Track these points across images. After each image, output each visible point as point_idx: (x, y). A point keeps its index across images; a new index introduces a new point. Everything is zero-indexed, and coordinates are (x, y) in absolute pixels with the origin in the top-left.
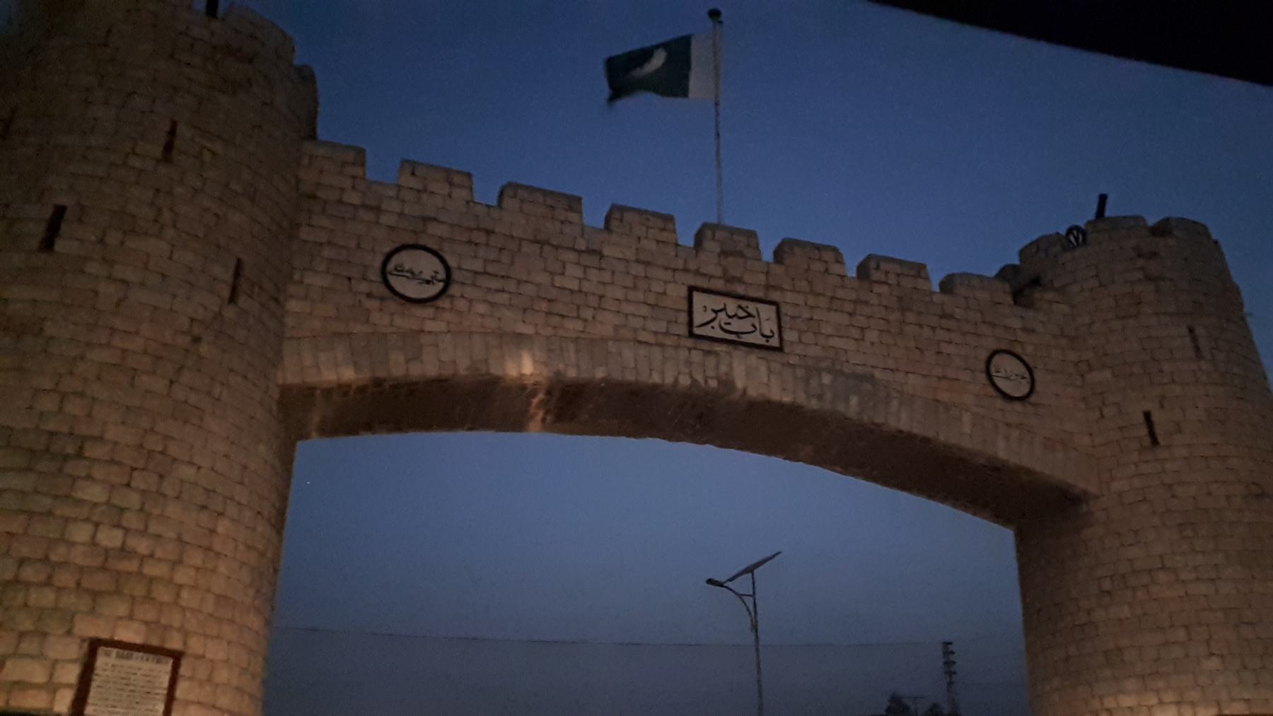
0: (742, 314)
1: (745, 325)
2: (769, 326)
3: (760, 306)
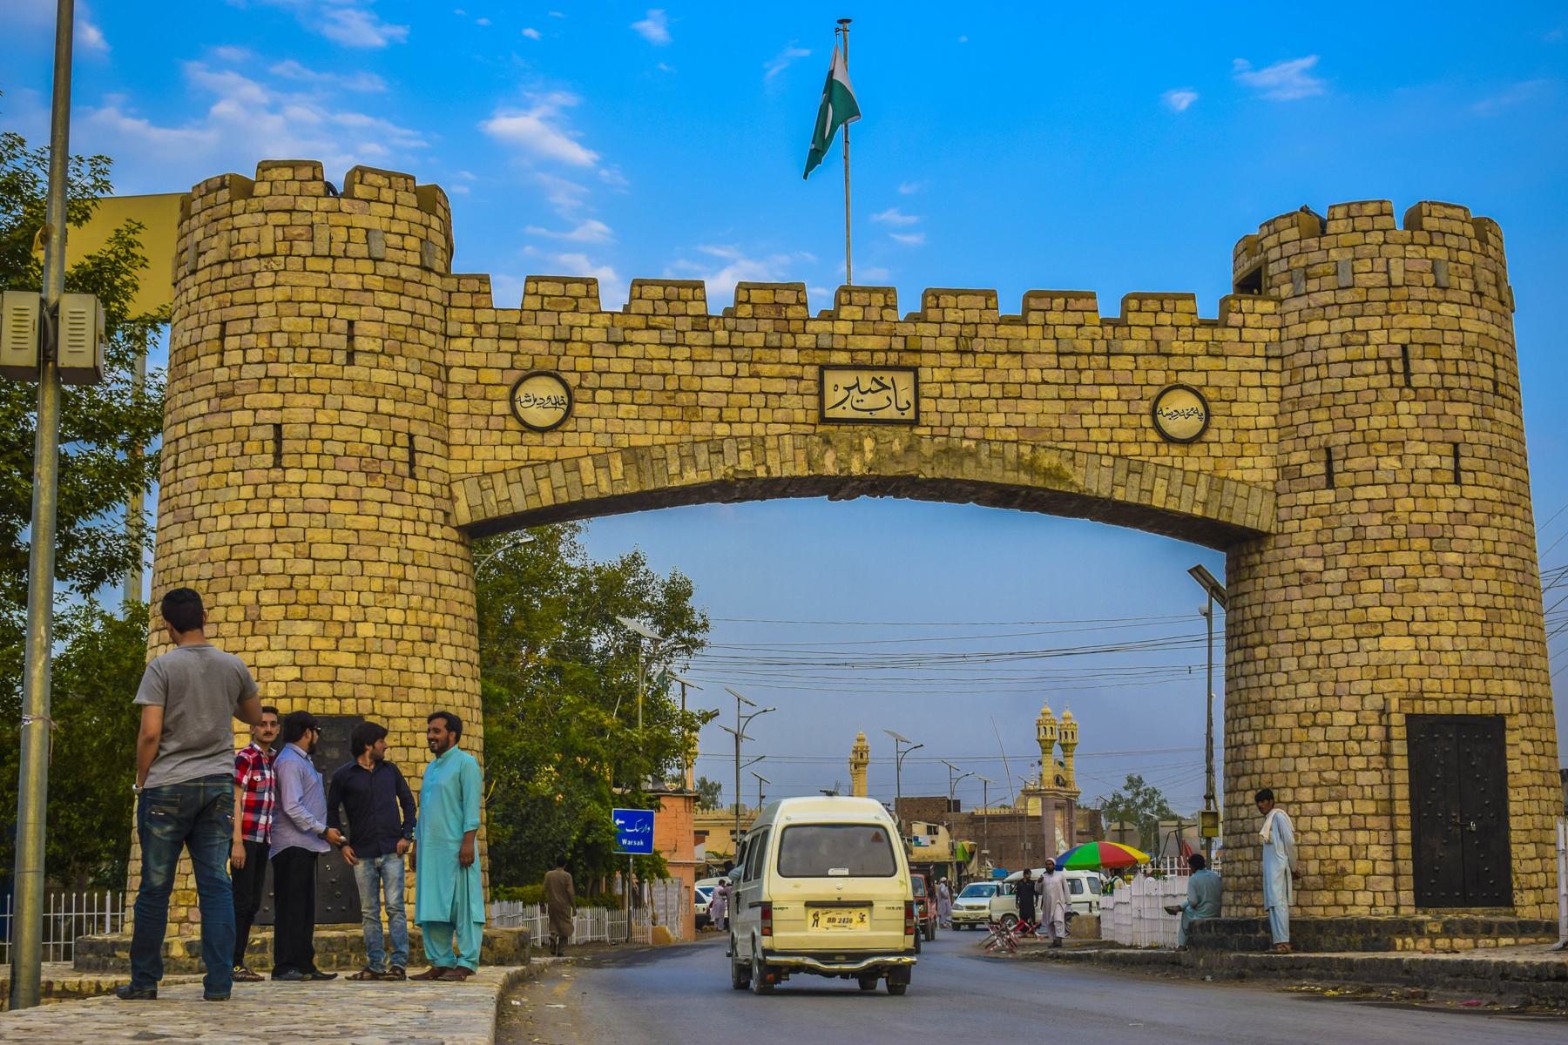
0: (876, 387)
1: (880, 399)
2: (906, 395)
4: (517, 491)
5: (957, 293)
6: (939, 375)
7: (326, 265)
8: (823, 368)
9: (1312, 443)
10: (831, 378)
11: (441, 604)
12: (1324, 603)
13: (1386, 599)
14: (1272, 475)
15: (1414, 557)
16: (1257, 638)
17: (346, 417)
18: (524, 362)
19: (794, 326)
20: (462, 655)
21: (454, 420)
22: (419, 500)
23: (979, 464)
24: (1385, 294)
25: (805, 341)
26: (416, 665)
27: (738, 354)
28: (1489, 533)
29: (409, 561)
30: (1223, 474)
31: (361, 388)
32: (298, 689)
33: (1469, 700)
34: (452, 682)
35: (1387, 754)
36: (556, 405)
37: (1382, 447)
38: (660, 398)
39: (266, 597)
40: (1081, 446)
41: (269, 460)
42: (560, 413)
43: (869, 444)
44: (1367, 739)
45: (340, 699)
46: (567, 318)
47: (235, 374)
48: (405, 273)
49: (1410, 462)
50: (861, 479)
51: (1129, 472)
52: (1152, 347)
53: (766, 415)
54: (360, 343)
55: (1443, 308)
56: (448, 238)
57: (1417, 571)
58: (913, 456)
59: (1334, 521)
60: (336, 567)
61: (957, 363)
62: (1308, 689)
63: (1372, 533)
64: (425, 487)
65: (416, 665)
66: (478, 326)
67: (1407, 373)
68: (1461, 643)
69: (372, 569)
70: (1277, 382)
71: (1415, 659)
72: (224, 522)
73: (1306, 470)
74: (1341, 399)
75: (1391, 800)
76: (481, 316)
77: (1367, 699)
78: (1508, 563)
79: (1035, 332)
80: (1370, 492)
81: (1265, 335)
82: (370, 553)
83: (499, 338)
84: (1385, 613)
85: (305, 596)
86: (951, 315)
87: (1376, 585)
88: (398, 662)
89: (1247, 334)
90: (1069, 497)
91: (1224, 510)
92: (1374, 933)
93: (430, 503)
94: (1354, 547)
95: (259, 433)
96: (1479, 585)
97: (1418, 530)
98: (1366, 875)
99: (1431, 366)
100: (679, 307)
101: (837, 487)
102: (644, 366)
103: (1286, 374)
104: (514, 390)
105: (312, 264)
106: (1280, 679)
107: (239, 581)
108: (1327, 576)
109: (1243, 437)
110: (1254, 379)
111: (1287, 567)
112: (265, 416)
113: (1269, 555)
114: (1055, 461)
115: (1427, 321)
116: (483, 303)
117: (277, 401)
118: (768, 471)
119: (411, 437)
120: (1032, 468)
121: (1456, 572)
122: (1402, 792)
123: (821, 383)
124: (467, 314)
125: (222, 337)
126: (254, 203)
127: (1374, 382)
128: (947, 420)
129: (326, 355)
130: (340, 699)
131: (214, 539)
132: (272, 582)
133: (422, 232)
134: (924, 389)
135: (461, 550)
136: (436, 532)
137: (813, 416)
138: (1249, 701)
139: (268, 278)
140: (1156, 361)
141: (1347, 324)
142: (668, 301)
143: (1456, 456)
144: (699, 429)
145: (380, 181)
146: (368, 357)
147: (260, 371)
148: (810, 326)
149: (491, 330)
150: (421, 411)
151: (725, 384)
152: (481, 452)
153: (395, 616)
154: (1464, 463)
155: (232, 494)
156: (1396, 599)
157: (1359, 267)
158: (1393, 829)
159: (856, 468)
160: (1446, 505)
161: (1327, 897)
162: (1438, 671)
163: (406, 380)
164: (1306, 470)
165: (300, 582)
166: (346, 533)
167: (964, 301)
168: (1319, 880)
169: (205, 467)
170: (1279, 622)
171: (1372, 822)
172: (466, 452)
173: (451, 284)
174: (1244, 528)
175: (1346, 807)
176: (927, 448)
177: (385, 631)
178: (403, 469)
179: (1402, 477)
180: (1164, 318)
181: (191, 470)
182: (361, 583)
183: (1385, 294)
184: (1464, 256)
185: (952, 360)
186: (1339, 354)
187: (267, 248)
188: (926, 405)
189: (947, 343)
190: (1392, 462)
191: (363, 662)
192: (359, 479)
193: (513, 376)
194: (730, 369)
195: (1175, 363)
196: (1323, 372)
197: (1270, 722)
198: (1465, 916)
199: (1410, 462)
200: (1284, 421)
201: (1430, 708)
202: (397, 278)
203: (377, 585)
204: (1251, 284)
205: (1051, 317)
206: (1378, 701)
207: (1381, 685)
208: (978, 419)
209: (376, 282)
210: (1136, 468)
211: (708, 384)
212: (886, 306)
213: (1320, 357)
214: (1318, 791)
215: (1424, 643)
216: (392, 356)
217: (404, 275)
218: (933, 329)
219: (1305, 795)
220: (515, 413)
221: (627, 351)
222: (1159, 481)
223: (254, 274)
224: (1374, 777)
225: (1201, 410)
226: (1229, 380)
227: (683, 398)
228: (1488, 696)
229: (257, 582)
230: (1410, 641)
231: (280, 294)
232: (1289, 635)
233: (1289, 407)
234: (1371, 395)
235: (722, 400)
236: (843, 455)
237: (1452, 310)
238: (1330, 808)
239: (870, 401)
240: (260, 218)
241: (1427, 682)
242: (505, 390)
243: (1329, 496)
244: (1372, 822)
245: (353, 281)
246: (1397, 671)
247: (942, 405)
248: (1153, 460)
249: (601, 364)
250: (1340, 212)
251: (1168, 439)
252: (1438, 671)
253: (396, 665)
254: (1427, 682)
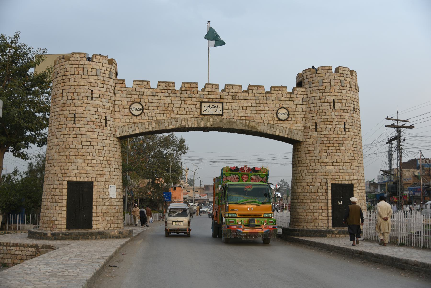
1: (214, 110)
2: (220, 109)
3: (218, 104)
4: (130, 129)
5: (232, 85)
6: (228, 104)
7: (87, 77)
8: (201, 102)
9: (312, 121)
10: (203, 104)
11: (112, 155)
12: (314, 158)
13: (328, 157)
14: (303, 128)
15: (334, 148)
16: (299, 165)
17: (90, 112)
18: (133, 100)
19: (195, 92)
20: (117, 167)
21: (116, 113)
22: (107, 132)
23: (236, 125)
24: (330, 88)
25: (197, 96)
26: (106, 169)
27: (182, 99)
28: (351, 143)
29: (105, 145)
31: (94, 106)
32: (79, 175)
33: (346, 180)
34: (115, 173)
35: (327, 193)
36: (140, 110)
37: (328, 123)
38: (164, 109)
39: (71, 154)
40: (260, 121)
41: (72, 122)
42: (141, 112)
43: (211, 120)
44: (322, 189)
45: (88, 177)
46: (143, 90)
47: (65, 102)
48: (105, 79)
49: (334, 126)
50: (210, 128)
51: (271, 127)
52: (277, 99)
53: (188, 113)
54: (94, 95)
55: (343, 91)
56: (116, 71)
57: (335, 151)
58: (222, 123)
59: (317, 139)
60: (87, 147)
61: (232, 102)
62: (310, 177)
63: (325, 142)
64: (109, 128)
65: (106, 169)
66: (122, 91)
67: (334, 106)
68: (344, 168)
69: (96, 147)
70: (305, 107)
71: (334, 171)
72: (62, 136)
73: (311, 127)
74: (319, 111)
75: (327, 203)
76: (123, 89)
77: (323, 180)
78: (355, 149)
79: (250, 95)
80: (325, 133)
81: (302, 96)
82: (95, 144)
83: (127, 94)
84: (327, 160)
85: (80, 154)
86: (231, 91)
87: (326, 154)
88: (102, 169)
89: (298, 96)
90: (257, 132)
91: (292, 136)
92: (322, 234)
93: (110, 132)
94: (321, 145)
95: (70, 116)
96: (349, 154)
97: (335, 142)
98: (321, 220)
99: (340, 104)
100: (169, 88)
101: (206, 129)
102: (160, 101)
103: (307, 105)
104: (130, 106)
105: (83, 77)
106: (304, 175)
107: (65, 150)
108: (315, 152)
109: (297, 119)
110: (300, 106)
111: (306, 149)
112: (72, 112)
113: (302, 146)
114: (254, 124)
115: (339, 94)
116: (123, 86)
117: (74, 108)
118: (188, 126)
119: (106, 117)
120: (248, 126)
121: (344, 151)
122: (330, 201)
123: (201, 106)
124: (120, 89)
125: (62, 93)
126: (70, 62)
127: (327, 108)
128: (230, 115)
129: (86, 98)
130: (88, 177)
131: (60, 140)
132: (73, 150)
133: (109, 70)
134: (224, 107)
135: (118, 143)
136: (111, 139)
137: (199, 113)
138: (297, 179)
139: (73, 80)
140: (277, 102)
141: (321, 94)
142: (166, 86)
143: (345, 125)
144: (172, 116)
145: (100, 57)
146: (96, 99)
147: (71, 101)
148: (199, 92)
149: (125, 92)
150: (108, 111)
151: (179, 106)
152: (122, 121)
153: (101, 158)
154: (346, 127)
155: (64, 129)
156: (330, 157)
157: (324, 81)
158: (328, 209)
159: (209, 125)
160: (342, 136)
161: (312, 224)
162: (339, 174)
163: (105, 104)
164: (311, 127)
165: (79, 150)
166: (90, 139)
167: (234, 87)
168: (311, 220)
169: (58, 123)
170: (304, 162)
171: (323, 208)
172: (119, 120)
173: (116, 82)
174: (296, 140)
175: (317, 204)
176: (225, 121)
177: (99, 162)
178: (104, 124)
179: (332, 130)
180: (280, 92)
181: (55, 124)
182: (93, 151)
183: (330, 88)
184: (348, 79)
185: (231, 101)
186: (319, 101)
187: (73, 73)
188: (225, 111)
189: (230, 97)
190: (330, 126)
191: (93, 169)
192: (93, 127)
193: (130, 103)
194: (180, 102)
195: (282, 102)
196: (315, 105)
197: (301, 184)
198: (343, 229)
199: (334, 126)
200: (306, 116)
201: (337, 182)
203: (97, 151)
204: (300, 84)
205: (254, 91)
206: (325, 180)
207: (326, 177)
208: (237, 114)
209: (98, 81)
210: (272, 126)
211: (175, 105)
212: (216, 88)
213: (315, 101)
214: (311, 200)
215: (336, 167)
216: (101, 98)
217: (105, 80)
218: (227, 94)
219: (308, 201)
220: (130, 112)
221: (156, 97)
222: (277, 129)
223: (70, 79)
224: (324, 198)
225: (287, 113)
226: (294, 106)
227: (169, 109)
228: (350, 180)
229: (69, 150)
230: (333, 167)
231: (76, 83)
232: (306, 165)
233: (307, 113)
234: (326, 111)
235: (178, 109)
236: (205, 122)
237: (345, 91)
238: (314, 204)
239: (212, 110)
240: (71, 66)
241: (336, 176)
242: (128, 106)
243: (316, 133)
244: (323, 208)
245: (93, 81)
246: (330, 174)
247: (229, 111)
249: (150, 101)
250: (320, 69)
251: (280, 120)
252: (339, 174)
253: (101, 170)
254: (336, 176)
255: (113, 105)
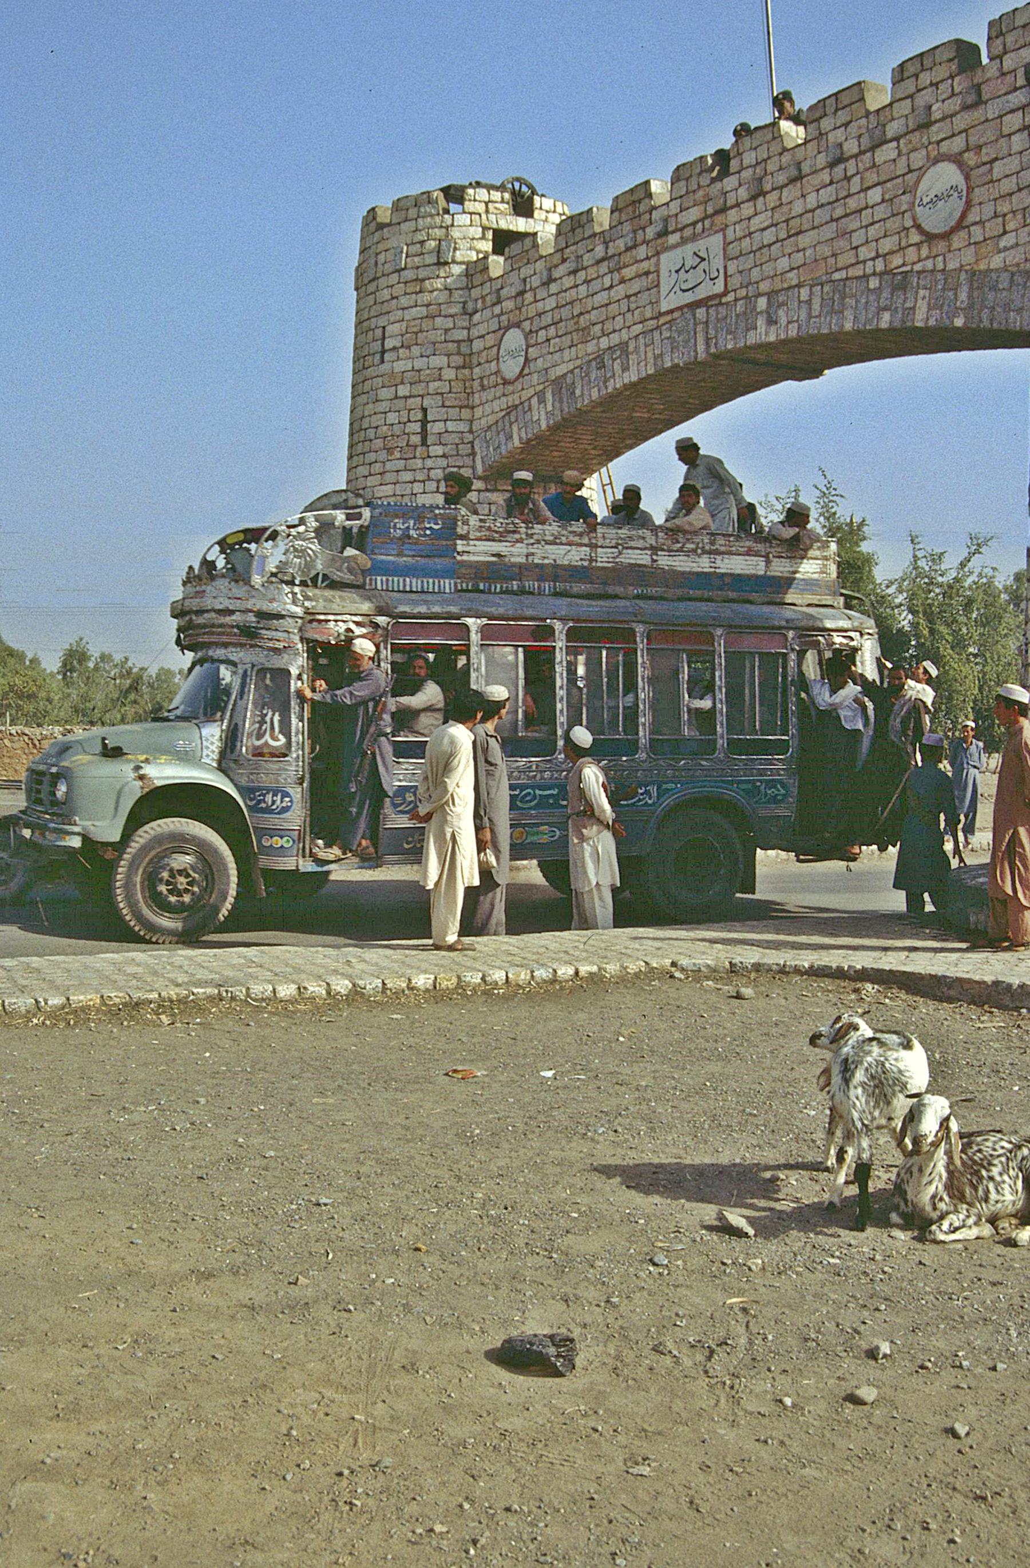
22: (429, 463)
30: (982, 267)
64: (439, 450)
93: (443, 462)
109: (1004, 207)
119: (425, 410)
150: (433, 386)
163: (419, 364)
178: (416, 439)
192: (383, 455)
195: (937, 132)
202: (416, 280)
216: (409, 347)
248: (918, 267)
255: (458, 360)
